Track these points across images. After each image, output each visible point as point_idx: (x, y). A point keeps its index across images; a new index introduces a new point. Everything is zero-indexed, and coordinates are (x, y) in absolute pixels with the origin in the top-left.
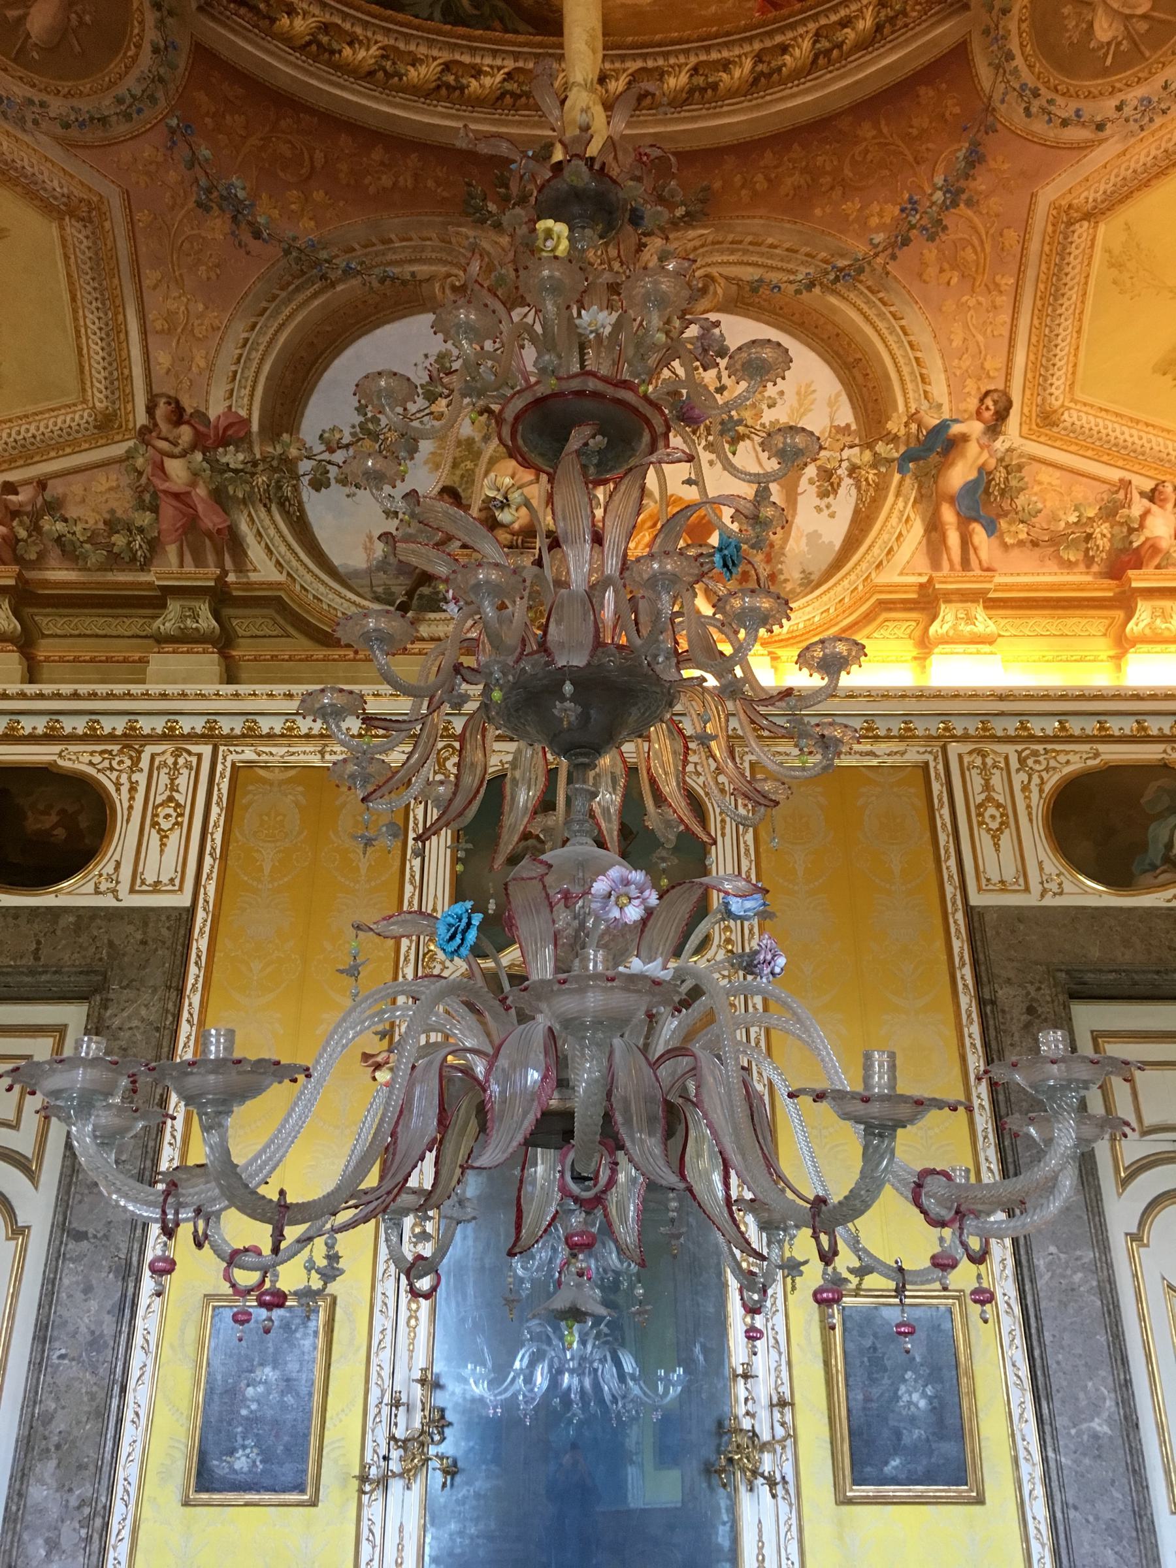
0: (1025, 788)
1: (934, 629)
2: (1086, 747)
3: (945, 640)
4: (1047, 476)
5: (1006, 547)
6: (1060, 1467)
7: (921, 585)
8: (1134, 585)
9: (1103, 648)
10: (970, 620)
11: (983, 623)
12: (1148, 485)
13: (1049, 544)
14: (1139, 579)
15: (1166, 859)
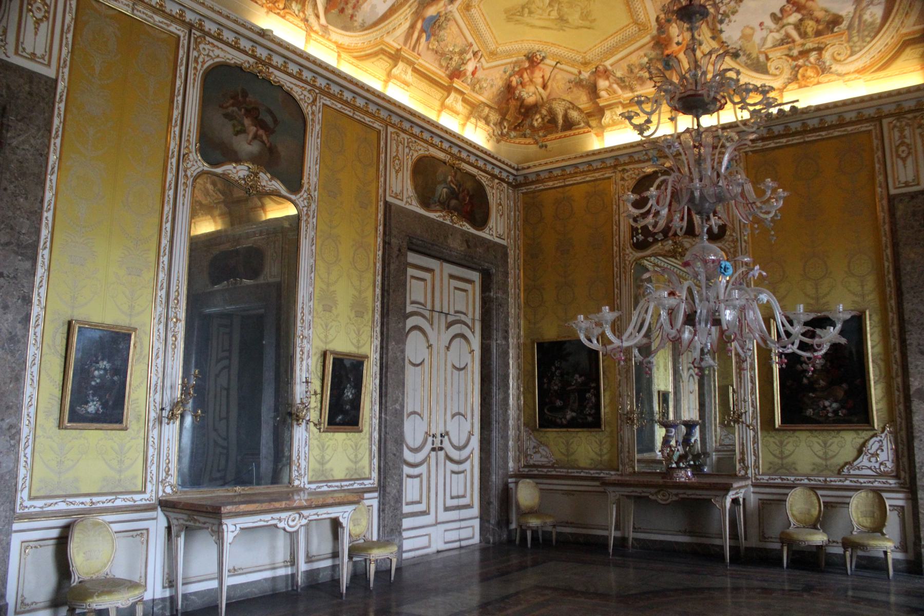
0: (408, 154)
1: (395, 71)
2: (425, 145)
3: (396, 78)
4: (454, 29)
5: (428, 48)
6: (386, 420)
7: (398, 50)
8: (454, 85)
9: (437, 104)
10: (406, 72)
11: (409, 76)
12: (476, 49)
13: (440, 54)
14: (457, 84)
15: (439, 201)
